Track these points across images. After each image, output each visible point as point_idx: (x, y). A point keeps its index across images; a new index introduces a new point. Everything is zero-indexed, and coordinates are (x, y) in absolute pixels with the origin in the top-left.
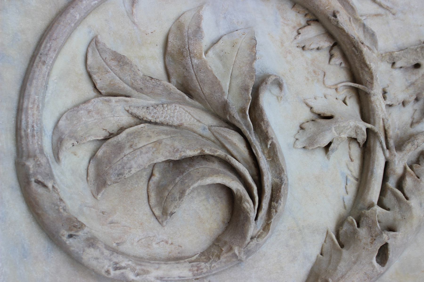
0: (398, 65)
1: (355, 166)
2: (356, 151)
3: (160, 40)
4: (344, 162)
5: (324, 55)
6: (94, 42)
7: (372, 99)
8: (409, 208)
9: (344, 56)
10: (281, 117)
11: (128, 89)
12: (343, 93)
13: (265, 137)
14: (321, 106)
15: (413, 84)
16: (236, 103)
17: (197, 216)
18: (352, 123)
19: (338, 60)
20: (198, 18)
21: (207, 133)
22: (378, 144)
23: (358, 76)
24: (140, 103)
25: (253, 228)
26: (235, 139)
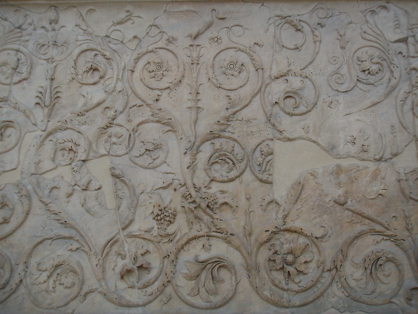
0: (192, 227)
1: (214, 238)
2: (211, 238)
3: (188, 281)
4: (213, 241)
5: (190, 245)
6: (189, 295)
7: (200, 235)
8: (223, 228)
9: (190, 241)
10: (204, 256)
11: (198, 288)
12: (198, 241)
13: (208, 260)
14: (201, 247)
15: (196, 223)
16: (201, 266)
17: (224, 274)
18: (205, 241)
19: (191, 242)
20: (184, 273)
21: (207, 271)
22: (210, 234)
23: (195, 238)
24: (201, 285)
25: (226, 264)
26: (208, 266)
